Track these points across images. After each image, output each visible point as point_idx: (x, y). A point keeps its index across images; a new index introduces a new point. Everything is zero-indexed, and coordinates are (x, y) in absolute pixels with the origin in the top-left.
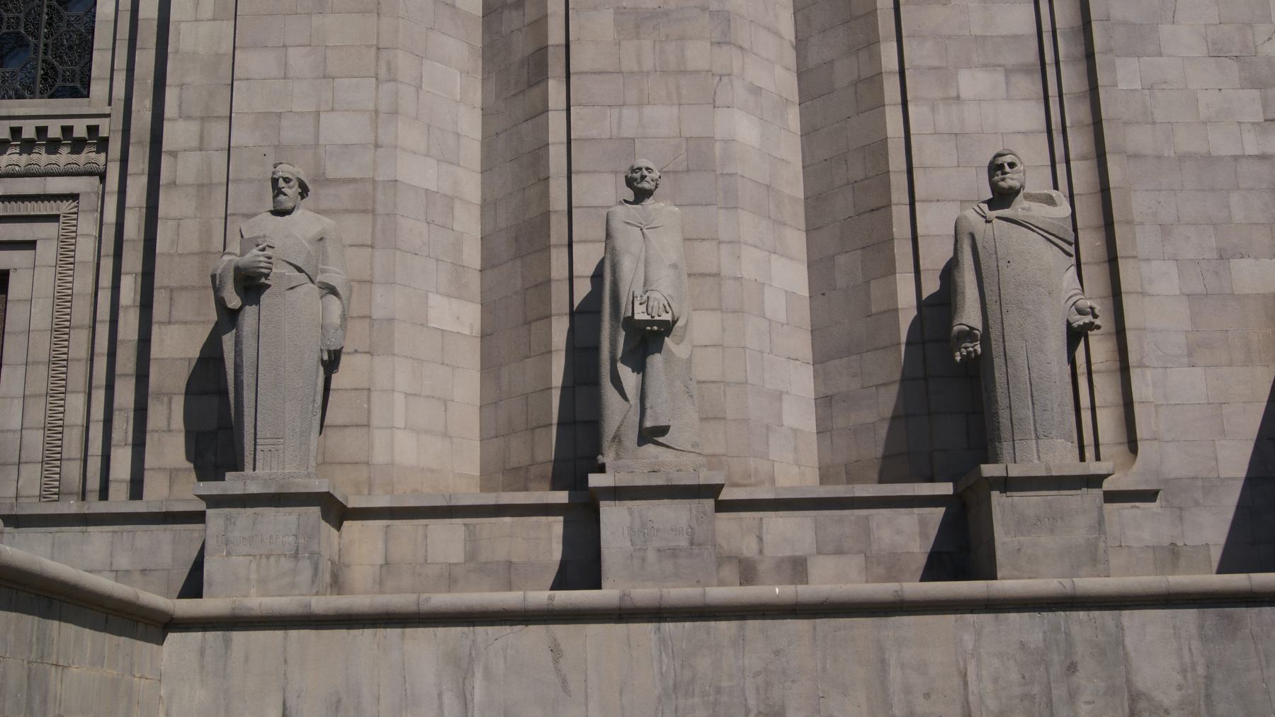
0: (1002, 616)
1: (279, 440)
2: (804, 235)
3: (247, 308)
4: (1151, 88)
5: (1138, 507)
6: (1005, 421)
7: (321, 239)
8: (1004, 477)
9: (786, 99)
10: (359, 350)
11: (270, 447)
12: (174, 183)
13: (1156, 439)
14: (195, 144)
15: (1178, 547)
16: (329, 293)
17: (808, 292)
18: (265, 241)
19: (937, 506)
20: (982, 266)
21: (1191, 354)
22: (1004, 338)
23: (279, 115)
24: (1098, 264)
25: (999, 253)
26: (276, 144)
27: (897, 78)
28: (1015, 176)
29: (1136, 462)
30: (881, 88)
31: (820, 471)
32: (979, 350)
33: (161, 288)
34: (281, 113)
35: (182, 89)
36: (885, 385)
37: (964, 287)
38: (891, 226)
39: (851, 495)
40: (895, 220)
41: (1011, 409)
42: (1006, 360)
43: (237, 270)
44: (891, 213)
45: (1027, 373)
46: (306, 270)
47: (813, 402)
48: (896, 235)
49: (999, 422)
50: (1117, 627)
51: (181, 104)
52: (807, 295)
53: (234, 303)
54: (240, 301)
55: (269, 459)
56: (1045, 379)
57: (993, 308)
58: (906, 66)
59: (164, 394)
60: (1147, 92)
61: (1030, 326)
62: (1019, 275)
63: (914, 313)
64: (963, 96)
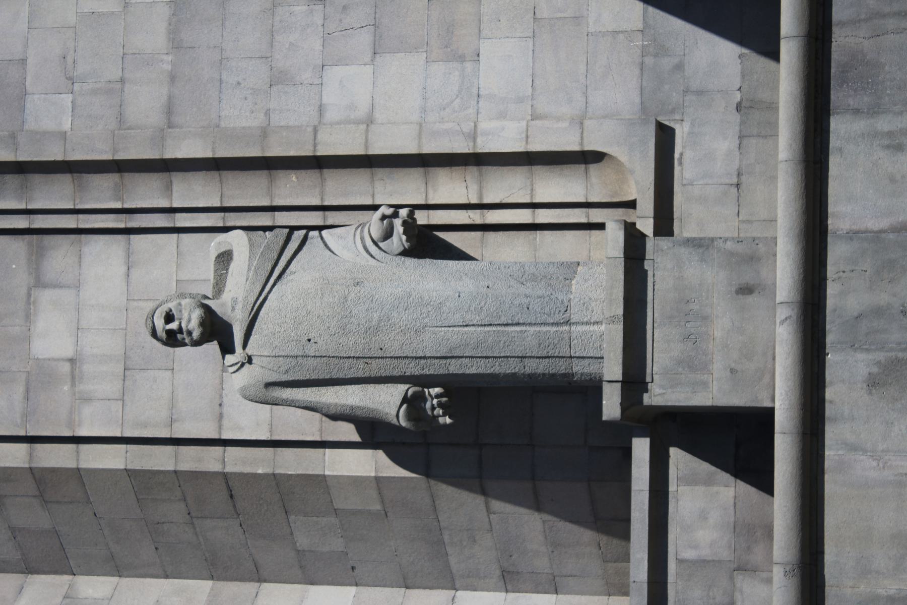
0: (829, 411)
2: (265, 585)
4: (72, 80)
5: (681, 155)
6: (541, 367)
8: (622, 387)
9: (65, 597)
13: (582, 123)
15: (742, 100)
17: (348, 588)
19: (667, 456)
20: (313, 378)
21: (460, 57)
22: (421, 358)
24: (323, 180)
25: (295, 353)
27: (38, 446)
28: (185, 315)
29: (613, 155)
30: (53, 470)
31: (614, 595)
37: (342, 406)
38: (255, 476)
39: (645, 586)
40: (247, 469)
41: (525, 357)
44: (235, 474)
47: (511, 595)
48: (269, 470)
49: (544, 374)
50: (851, 239)
52: (353, 589)
56: (482, 304)
57: (376, 368)
58: (22, 433)
60: (77, 87)
61: (404, 318)
63: (380, 454)
64: (69, 353)
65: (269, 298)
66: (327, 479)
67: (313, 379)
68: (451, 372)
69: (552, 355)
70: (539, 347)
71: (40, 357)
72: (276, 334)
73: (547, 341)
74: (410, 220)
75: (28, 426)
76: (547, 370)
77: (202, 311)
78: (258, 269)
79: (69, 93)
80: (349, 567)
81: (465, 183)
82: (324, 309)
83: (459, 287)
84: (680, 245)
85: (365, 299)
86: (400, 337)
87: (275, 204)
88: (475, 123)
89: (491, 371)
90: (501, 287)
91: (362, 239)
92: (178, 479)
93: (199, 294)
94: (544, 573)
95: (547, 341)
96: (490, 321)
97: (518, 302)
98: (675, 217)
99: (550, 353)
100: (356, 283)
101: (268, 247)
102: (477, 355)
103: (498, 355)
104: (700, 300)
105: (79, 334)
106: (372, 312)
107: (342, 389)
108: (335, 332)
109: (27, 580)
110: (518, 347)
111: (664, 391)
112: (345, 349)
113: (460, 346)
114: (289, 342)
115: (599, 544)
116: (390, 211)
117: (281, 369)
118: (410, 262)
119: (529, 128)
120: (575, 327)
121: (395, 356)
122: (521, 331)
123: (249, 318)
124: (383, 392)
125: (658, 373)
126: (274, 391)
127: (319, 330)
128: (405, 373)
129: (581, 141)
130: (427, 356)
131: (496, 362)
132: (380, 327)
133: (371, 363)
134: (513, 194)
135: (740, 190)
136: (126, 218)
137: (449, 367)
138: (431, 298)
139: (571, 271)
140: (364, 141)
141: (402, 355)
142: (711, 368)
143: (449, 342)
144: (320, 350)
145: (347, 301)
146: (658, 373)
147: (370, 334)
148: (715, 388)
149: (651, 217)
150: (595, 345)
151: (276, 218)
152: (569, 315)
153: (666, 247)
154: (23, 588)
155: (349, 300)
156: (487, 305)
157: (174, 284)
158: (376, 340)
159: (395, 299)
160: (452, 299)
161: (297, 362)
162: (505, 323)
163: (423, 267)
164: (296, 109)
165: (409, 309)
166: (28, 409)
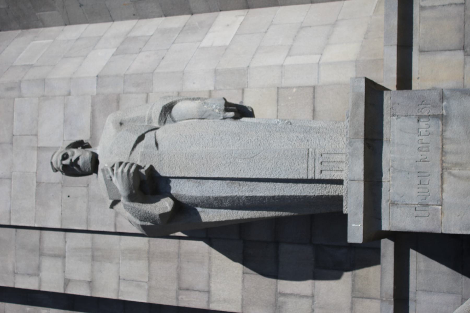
1: (310, 155)
3: (172, 192)
7: (121, 124)
10: (240, 100)
11: (318, 163)
12: (90, 282)
14: (59, 262)
16: (170, 112)
18: (107, 170)
23: (39, 184)
26: (60, 185)
33: (177, 299)
34: (37, 182)
35: (17, 273)
43: (132, 198)
46: (143, 132)
51: (28, 274)
53: (168, 205)
54: (166, 199)
55: (331, 164)
59: (276, 300)
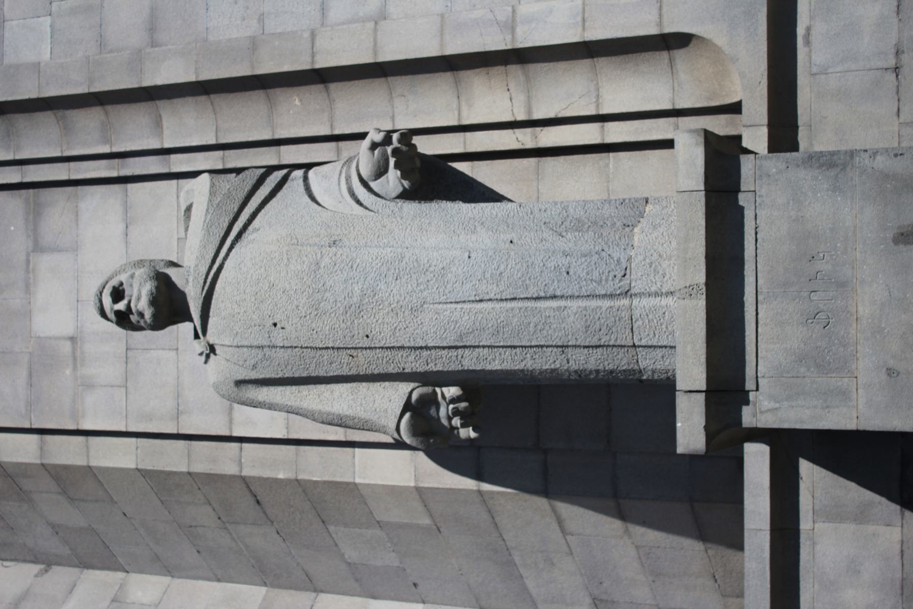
5: (808, 29)
6: (592, 360)
9: (114, 600)
20: (286, 376)
22: (421, 348)
24: (332, 101)
29: (705, 36)
30: (66, 467)
32: (452, 391)
36: (560, 522)
38: (276, 481)
40: (267, 473)
41: (567, 346)
42: (465, 347)
44: (254, 477)
45: (490, 305)
48: (290, 475)
49: (597, 371)
56: (502, 267)
57: (364, 363)
58: (27, 425)
61: (395, 291)
62: (297, 307)
64: (69, 331)
65: (225, 266)
66: (360, 487)
67: (288, 378)
68: (466, 368)
69: (606, 344)
70: (586, 331)
71: (41, 335)
72: (236, 316)
73: (598, 323)
74: (404, 148)
75: (32, 417)
76: (602, 365)
77: (151, 285)
78: (211, 227)
79: (47, 16)
80: (411, 584)
81: (508, 93)
82: (291, 281)
83: (471, 244)
84: (798, 166)
85: (343, 265)
86: (390, 319)
87: (277, 136)
88: (513, 7)
89: (521, 366)
90: (529, 241)
91: (348, 179)
92: (195, 482)
93: (162, 260)
94: (646, 604)
95: (598, 323)
96: (513, 294)
97: (552, 264)
98: (800, 123)
99: (603, 341)
100: (332, 242)
101: (228, 195)
102: (497, 344)
103: (528, 344)
104: (833, 255)
105: (79, 307)
106: (352, 283)
107: (327, 390)
108: (306, 312)
109: (82, 576)
110: (555, 332)
111: (777, 405)
112: (320, 337)
113: (473, 331)
114: (252, 327)
115: (714, 576)
116: (378, 137)
117: (248, 363)
118: (411, 208)
119: (586, 8)
120: (638, 300)
121: (387, 345)
122: (559, 308)
123: (202, 294)
124: (379, 395)
125: (767, 375)
126: (248, 391)
127: (286, 310)
128: (404, 369)
129: (659, 20)
130: (429, 345)
131: (526, 354)
132: (363, 305)
133: (357, 356)
134: (572, 104)
135: (899, 77)
136: (118, 165)
137: (463, 360)
138: (430, 261)
139: (635, 213)
140: (372, 44)
141: (395, 344)
142: (854, 367)
143: (458, 325)
144: (289, 338)
145: (320, 267)
146: (767, 375)
147: (351, 315)
148: (862, 401)
149: (763, 125)
150: (670, 329)
151: (282, 154)
152: (628, 282)
153: (774, 170)
154: (75, 586)
155: (322, 267)
156: (509, 270)
157: (175, 243)
158: (359, 324)
159: (382, 265)
160: (459, 261)
161: (265, 355)
162: (534, 296)
163: (426, 215)
164: (293, 10)
165: (401, 278)
166: (32, 397)
